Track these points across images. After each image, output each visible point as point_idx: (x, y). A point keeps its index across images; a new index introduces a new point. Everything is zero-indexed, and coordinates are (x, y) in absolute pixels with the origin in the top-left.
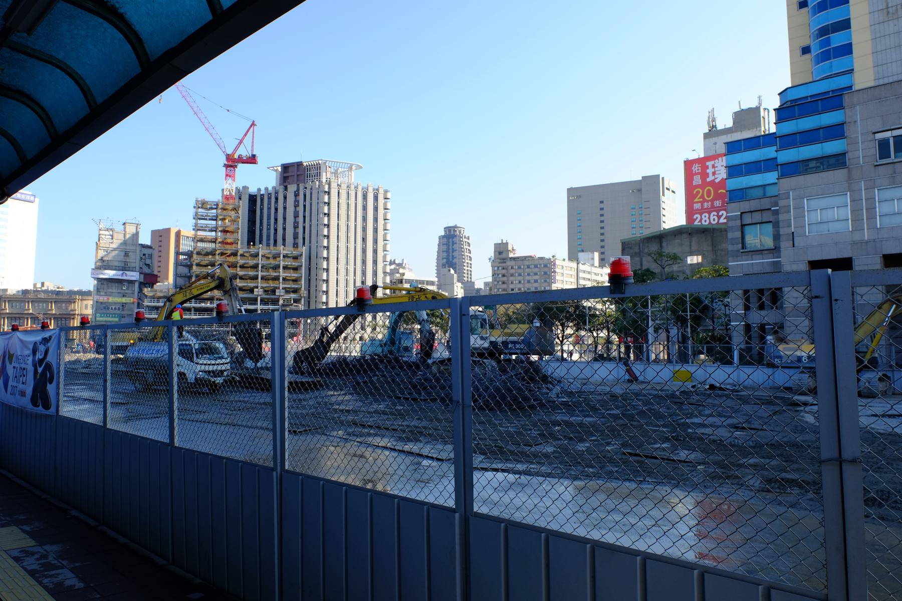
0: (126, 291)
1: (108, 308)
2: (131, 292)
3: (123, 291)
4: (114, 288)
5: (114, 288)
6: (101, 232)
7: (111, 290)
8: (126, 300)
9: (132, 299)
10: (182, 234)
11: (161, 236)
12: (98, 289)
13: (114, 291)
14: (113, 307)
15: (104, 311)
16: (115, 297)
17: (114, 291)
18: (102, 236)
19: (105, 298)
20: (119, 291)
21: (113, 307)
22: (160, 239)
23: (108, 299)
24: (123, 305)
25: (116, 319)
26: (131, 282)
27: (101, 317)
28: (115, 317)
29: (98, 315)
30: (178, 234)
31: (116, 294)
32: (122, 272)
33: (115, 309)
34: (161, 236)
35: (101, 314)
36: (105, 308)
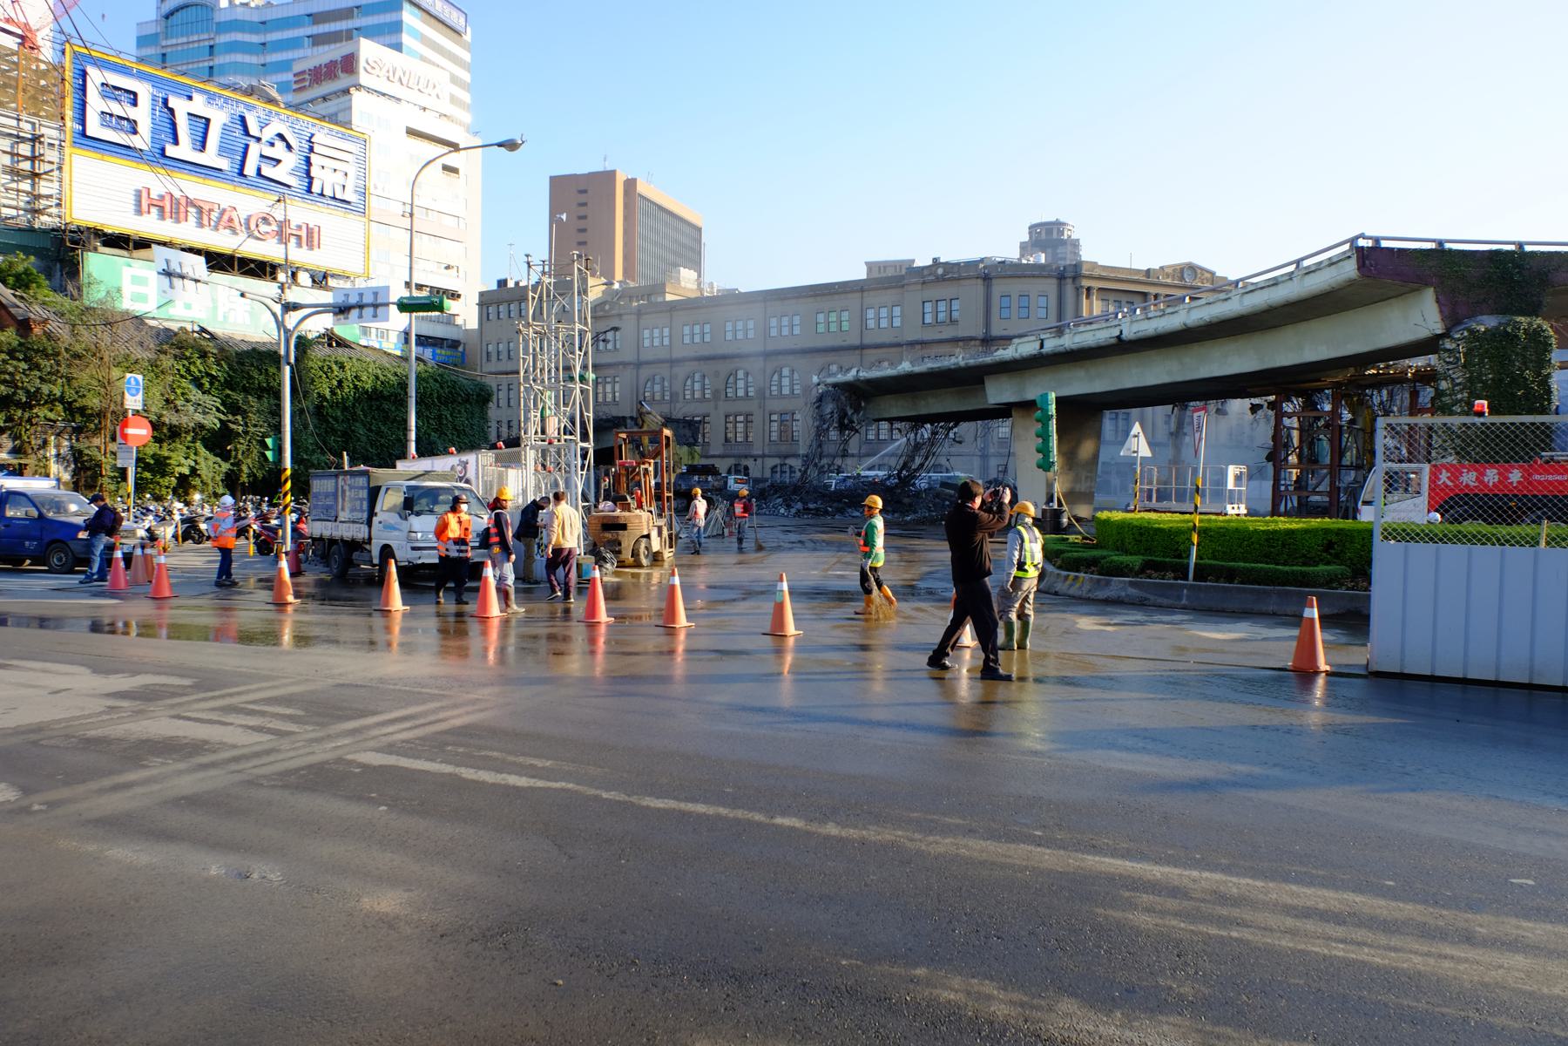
11: (585, 192)
22: (582, 198)
30: (630, 184)
34: (585, 192)
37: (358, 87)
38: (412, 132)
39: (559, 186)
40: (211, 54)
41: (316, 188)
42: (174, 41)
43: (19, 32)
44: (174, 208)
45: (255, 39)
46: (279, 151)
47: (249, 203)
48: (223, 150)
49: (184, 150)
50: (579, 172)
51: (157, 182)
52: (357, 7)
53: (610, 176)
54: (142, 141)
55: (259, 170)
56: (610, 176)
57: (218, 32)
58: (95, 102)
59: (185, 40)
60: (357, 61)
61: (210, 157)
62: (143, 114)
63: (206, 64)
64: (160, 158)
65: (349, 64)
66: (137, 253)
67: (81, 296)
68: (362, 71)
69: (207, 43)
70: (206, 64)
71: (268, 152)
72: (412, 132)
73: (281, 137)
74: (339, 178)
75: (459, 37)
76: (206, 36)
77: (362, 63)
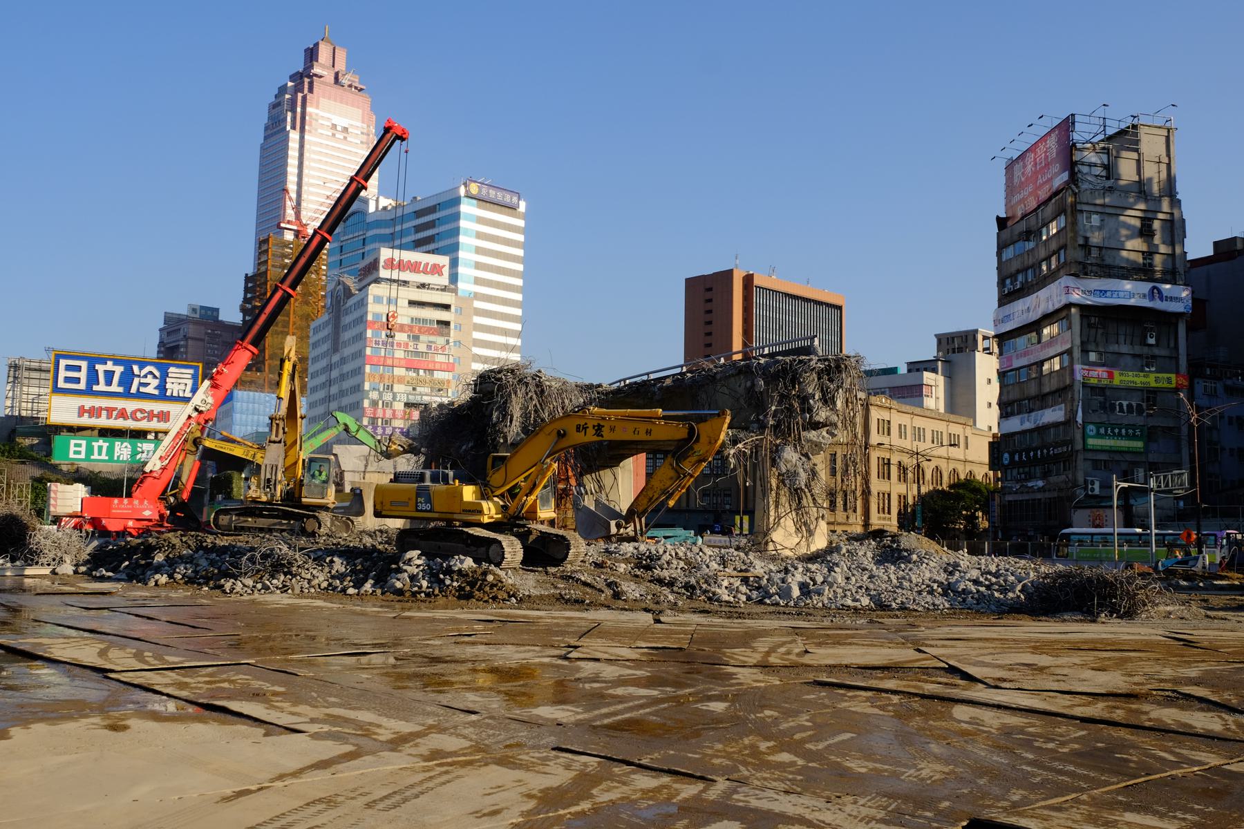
0: (1156, 351)
1: (1113, 407)
2: (1164, 352)
3: (1145, 350)
4: (1122, 339)
5: (1122, 339)
6: (1077, 156)
7: (1114, 348)
8: (1157, 380)
9: (1173, 376)
10: (757, 282)
11: (710, 289)
12: (1082, 343)
13: (1124, 349)
14: (1125, 403)
15: (1104, 418)
16: (1126, 368)
17: (1124, 349)
18: (1085, 169)
19: (1101, 372)
20: (1138, 350)
21: (1125, 403)
22: (709, 295)
23: (1111, 376)
24: (1151, 394)
25: (1139, 444)
26: (1165, 321)
27: (1098, 435)
28: (1134, 437)
29: (1091, 429)
30: (748, 280)
31: (1129, 360)
32: (1150, 285)
33: (1129, 406)
34: (710, 289)
35: (1098, 425)
36: (1103, 407)
37: (378, 281)
38: (412, 303)
39: (692, 284)
40: (364, 244)
41: (168, 393)
42: (346, 237)
43: (295, 228)
44: (95, 412)
45: (388, 231)
46: (149, 379)
47: (130, 405)
48: (120, 384)
49: (101, 387)
50: (706, 273)
51: (89, 402)
52: (439, 204)
53: (728, 275)
54: (82, 386)
55: (138, 389)
56: (728, 275)
57: (367, 230)
58: (63, 374)
59: (351, 236)
60: (379, 263)
61: (114, 388)
62: (83, 375)
63: (361, 251)
64: (89, 392)
65: (374, 266)
66: (77, 434)
67: (49, 454)
68: (381, 268)
69: (362, 237)
70: (361, 251)
71: (143, 380)
72: (412, 303)
73: (151, 373)
74: (182, 387)
75: (514, 211)
76: (361, 233)
77: (382, 263)
